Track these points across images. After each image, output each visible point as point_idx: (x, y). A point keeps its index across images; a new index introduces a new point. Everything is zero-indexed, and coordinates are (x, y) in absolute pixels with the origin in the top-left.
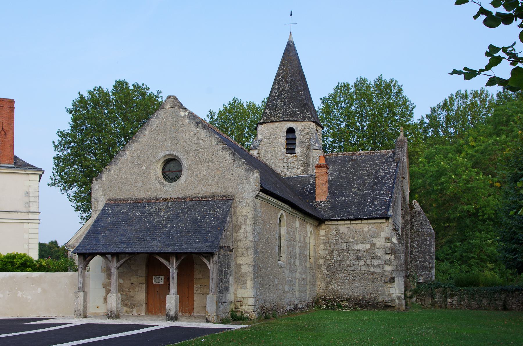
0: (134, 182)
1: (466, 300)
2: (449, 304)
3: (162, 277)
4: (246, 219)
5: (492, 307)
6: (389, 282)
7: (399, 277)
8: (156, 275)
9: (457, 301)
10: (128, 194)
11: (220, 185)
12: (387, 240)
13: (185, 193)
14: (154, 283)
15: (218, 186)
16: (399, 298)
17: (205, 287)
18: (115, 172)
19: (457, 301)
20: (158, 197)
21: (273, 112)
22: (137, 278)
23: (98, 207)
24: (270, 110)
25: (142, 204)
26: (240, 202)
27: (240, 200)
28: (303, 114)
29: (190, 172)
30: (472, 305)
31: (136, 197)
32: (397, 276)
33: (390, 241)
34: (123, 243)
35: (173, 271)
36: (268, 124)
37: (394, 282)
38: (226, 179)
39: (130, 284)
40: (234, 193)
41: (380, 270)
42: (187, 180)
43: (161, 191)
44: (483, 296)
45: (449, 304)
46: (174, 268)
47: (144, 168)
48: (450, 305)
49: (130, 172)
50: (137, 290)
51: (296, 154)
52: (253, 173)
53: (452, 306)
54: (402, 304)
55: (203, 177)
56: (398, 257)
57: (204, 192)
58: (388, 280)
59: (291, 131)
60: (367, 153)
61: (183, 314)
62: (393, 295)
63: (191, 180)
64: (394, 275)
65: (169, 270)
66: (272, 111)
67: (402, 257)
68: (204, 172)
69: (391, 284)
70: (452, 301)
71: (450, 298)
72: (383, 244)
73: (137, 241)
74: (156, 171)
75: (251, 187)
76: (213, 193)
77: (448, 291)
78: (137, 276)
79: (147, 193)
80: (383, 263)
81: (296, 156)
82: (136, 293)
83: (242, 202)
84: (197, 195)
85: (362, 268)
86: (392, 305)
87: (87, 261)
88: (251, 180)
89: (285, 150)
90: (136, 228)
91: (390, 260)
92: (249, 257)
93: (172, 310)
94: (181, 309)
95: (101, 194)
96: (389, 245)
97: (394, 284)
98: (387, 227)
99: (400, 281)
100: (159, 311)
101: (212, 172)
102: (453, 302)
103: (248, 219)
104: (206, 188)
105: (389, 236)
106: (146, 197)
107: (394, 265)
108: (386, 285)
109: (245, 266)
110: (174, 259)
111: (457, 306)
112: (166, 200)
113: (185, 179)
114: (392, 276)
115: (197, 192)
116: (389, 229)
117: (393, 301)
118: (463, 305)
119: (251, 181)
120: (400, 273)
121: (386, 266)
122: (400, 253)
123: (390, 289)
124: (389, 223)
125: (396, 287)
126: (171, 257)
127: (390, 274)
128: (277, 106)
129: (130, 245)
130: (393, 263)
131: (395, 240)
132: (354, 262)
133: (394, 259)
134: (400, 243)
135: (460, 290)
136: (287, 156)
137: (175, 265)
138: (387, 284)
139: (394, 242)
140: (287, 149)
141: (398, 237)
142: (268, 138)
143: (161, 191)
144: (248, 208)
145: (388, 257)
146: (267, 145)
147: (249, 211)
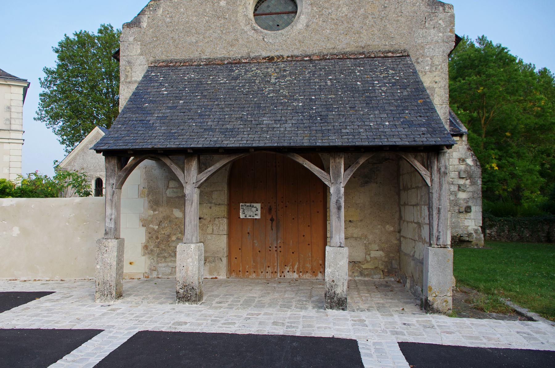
0: (203, 28)
1: (506, 231)
2: (488, 235)
3: (258, 206)
5: (534, 239)
6: (464, 213)
7: (476, 206)
8: (246, 203)
9: (496, 232)
10: (192, 52)
11: (376, 32)
12: (461, 161)
13: (305, 49)
14: (242, 216)
15: (372, 35)
16: (476, 231)
17: (350, 224)
18: (167, 12)
19: (496, 232)
20: (252, 55)
22: (210, 208)
23: (131, 77)
25: (225, 66)
26: (418, 63)
27: (418, 59)
29: (315, 8)
30: (513, 237)
31: (209, 57)
32: (474, 205)
33: (464, 163)
34: (210, 129)
35: (338, 191)
37: (470, 212)
38: (389, 20)
40: (407, 47)
41: (453, 197)
42: (310, 23)
43: (258, 45)
44: (524, 227)
45: (488, 235)
46: (343, 185)
48: (489, 236)
49: (197, 11)
50: (209, 230)
52: (444, 10)
53: (491, 237)
54: (481, 238)
55: (342, 17)
56: (474, 182)
57: (344, 46)
58: (463, 209)
61: (299, 276)
62: (470, 228)
63: (317, 23)
64: (470, 204)
65: (325, 188)
67: (479, 181)
68: (344, 9)
69: (467, 215)
70: (491, 232)
71: (488, 229)
72: (456, 166)
73: (242, 126)
74: (246, 8)
75: (441, 35)
76: (363, 48)
77: (487, 222)
78: (211, 203)
79: (230, 48)
80: (457, 188)
82: (209, 237)
83: (422, 63)
84: (331, 51)
86: (470, 240)
88: (440, 22)
90: (226, 102)
91: (465, 185)
93: (340, 283)
94: (296, 267)
95: (139, 51)
96: (463, 167)
97: (469, 214)
98: (460, 146)
99: (477, 212)
100: (252, 270)
101: (360, 9)
102: (492, 233)
103: (436, 95)
104: (348, 37)
105: (463, 157)
106: (227, 56)
107: (469, 192)
108: (461, 215)
110: (340, 163)
111: (496, 237)
112: (271, 59)
113: (305, 21)
114: (468, 205)
115: (329, 46)
116: (463, 148)
117: (470, 235)
118: (503, 237)
119: (440, 24)
120: (477, 201)
121: (460, 193)
122: (477, 177)
123: (466, 220)
124: (463, 141)
125: (472, 218)
126: (335, 158)
127: (465, 203)
129: (233, 132)
130: (468, 190)
131: (470, 161)
133: (469, 184)
134: (477, 165)
135: (501, 220)
137: (345, 178)
138: (461, 214)
139: (469, 165)
141: (473, 158)
143: (258, 45)
144: (435, 74)
145: (462, 182)
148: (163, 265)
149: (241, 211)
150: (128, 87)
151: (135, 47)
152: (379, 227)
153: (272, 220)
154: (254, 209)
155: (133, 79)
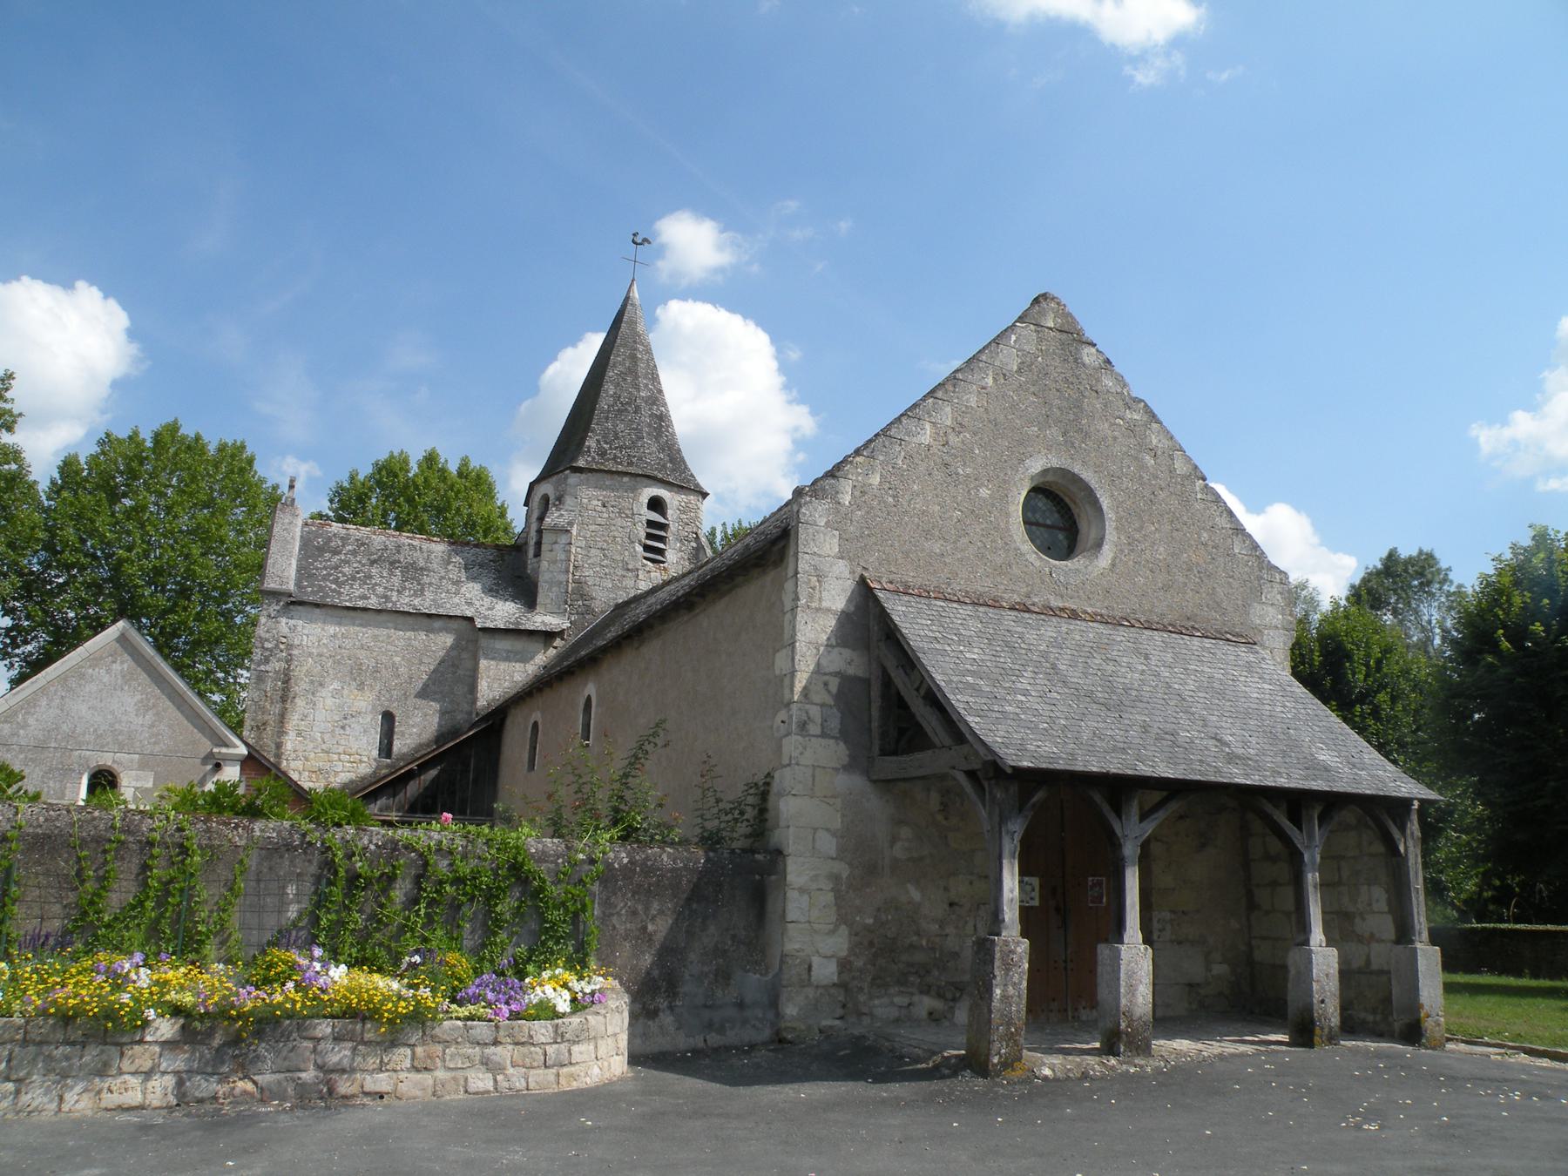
21: (611, 448)
22: (971, 883)
36: (599, 475)
39: (946, 906)
51: (666, 565)
59: (656, 504)
65: (1302, 854)
78: (972, 874)
81: (665, 569)
87: (1034, 805)
89: (640, 549)
128: (617, 438)
136: (644, 565)
140: (647, 548)
142: (599, 509)
146: (593, 527)
148: (885, 1000)
150: (814, 620)
151: (827, 538)
153: (1057, 909)
155: (824, 604)
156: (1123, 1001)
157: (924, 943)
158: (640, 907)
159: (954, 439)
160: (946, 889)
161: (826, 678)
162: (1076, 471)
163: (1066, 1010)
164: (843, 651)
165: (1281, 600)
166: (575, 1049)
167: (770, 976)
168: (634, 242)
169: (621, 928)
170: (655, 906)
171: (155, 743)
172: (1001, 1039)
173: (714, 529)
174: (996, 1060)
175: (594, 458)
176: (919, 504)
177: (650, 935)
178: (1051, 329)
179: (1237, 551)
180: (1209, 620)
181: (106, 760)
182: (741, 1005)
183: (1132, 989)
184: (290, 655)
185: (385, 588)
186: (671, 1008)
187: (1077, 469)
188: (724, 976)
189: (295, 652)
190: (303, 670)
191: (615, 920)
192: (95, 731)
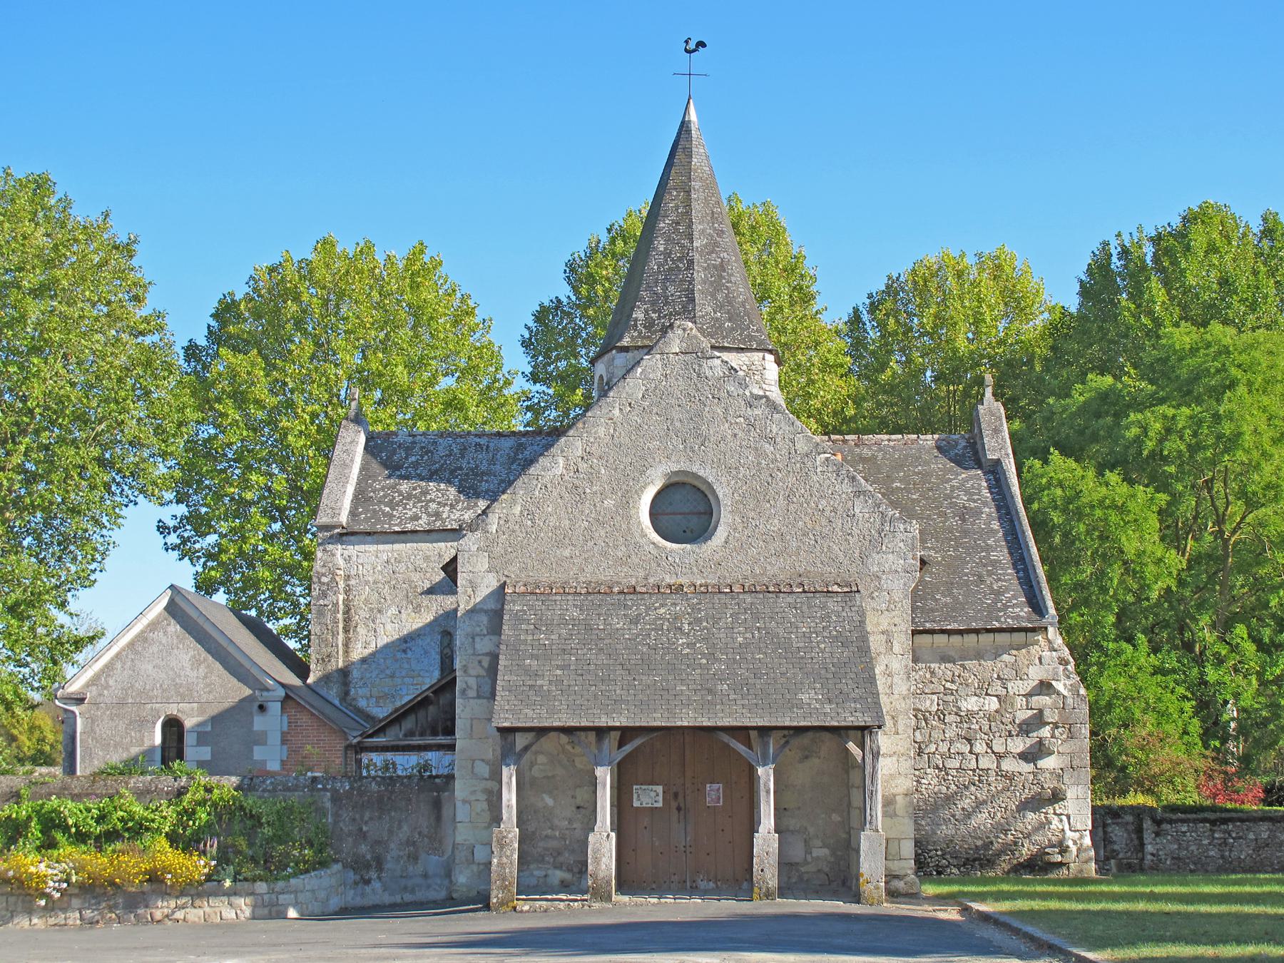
2: (1149, 857)
3: (660, 789)
4: (889, 642)
14: (636, 804)
21: (659, 318)
24: (646, 311)
28: (745, 330)
39: (574, 809)
47: (609, 503)
60: (899, 440)
66: (654, 316)
85: (980, 762)
92: (900, 737)
109: (889, 759)
132: (959, 745)
147: (897, 620)
149: (635, 796)
152: (823, 816)
153: (679, 809)
154: (653, 794)
156: (590, 868)
157: (557, 834)
158: (357, 816)
159: (583, 466)
160: (574, 797)
161: (480, 657)
162: (694, 470)
163: (685, 882)
164: (492, 637)
165: (903, 547)
166: (281, 897)
167: (445, 857)
168: (686, 50)
169: (346, 830)
170: (367, 815)
171: (210, 692)
172: (498, 889)
173: (1106, 244)
174: (495, 900)
175: (640, 333)
176: (553, 521)
177: (365, 833)
178: (677, 354)
179: (857, 511)
180: (822, 575)
181: (173, 710)
182: (425, 876)
183: (597, 861)
184: (348, 586)
185: (439, 503)
186: (379, 878)
187: (695, 469)
188: (414, 858)
189: (352, 582)
190: (363, 595)
191: (341, 824)
192: (161, 686)
